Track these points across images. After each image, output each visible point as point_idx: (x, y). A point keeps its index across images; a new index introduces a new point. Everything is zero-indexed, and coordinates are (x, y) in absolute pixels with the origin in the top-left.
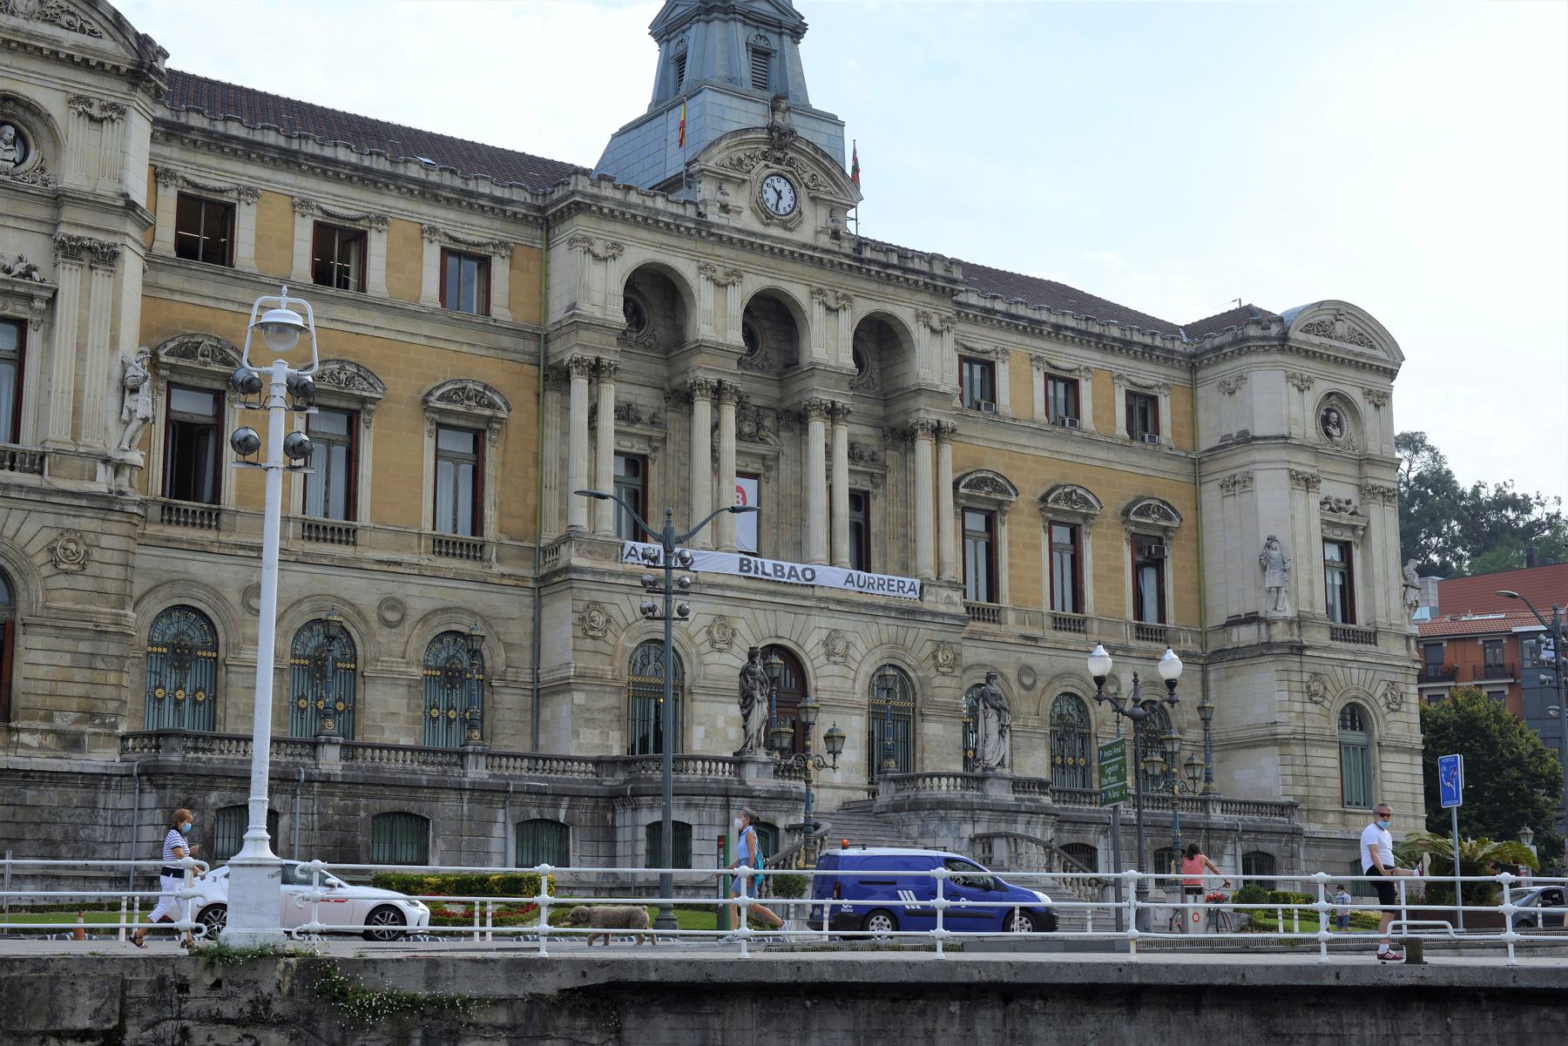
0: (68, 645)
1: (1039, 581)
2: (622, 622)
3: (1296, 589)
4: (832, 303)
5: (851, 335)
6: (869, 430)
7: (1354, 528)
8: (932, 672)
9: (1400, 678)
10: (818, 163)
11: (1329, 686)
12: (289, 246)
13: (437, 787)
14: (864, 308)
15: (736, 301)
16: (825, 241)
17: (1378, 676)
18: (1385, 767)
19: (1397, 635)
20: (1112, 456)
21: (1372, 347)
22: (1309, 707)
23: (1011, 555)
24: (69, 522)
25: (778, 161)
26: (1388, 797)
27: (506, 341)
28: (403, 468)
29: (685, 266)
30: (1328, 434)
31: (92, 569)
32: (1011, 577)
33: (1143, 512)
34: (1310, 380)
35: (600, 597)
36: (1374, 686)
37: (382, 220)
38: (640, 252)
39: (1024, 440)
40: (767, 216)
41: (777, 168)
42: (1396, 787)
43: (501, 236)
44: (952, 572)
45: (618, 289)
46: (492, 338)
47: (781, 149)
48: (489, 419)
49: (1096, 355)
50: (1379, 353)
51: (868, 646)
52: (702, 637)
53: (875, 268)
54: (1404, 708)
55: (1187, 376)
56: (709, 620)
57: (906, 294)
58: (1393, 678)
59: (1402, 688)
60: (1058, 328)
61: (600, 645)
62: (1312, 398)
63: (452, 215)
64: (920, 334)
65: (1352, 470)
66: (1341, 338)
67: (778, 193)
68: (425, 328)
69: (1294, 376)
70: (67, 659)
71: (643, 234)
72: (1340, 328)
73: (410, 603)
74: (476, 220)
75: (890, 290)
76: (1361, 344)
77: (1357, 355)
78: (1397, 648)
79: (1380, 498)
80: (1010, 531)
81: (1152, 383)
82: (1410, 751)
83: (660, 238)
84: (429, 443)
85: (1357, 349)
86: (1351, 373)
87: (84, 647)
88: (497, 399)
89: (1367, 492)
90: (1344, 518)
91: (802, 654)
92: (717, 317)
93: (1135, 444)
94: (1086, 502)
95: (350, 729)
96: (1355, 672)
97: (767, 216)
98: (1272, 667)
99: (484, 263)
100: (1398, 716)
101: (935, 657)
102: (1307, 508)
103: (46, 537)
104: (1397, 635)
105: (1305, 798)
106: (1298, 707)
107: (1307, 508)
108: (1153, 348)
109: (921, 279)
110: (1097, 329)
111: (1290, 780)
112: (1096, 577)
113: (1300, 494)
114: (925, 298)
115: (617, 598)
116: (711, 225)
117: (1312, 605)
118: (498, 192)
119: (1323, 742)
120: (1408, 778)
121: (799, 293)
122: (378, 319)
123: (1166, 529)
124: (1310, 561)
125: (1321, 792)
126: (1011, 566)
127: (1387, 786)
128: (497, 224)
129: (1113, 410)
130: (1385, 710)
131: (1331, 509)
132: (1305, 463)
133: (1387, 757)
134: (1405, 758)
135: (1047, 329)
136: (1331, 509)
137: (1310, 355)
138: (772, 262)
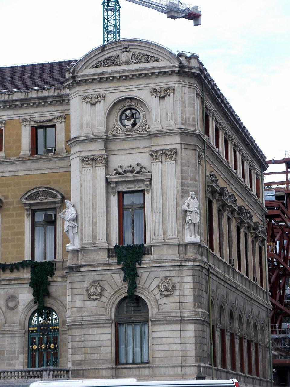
3: (82, 230)
7: (143, 181)
9: (174, 274)
11: (107, 287)
17: (153, 275)
18: (155, 335)
19: (170, 245)
20: (19, 168)
21: (158, 60)
22: (88, 303)
26: (157, 355)
30: (124, 126)
33: (35, 196)
34: (100, 96)
42: (166, 348)
49: (10, 112)
50: (163, 63)
54: (177, 293)
58: (167, 274)
59: (176, 280)
62: (102, 108)
65: (144, 143)
66: (127, 63)
69: (87, 96)
72: (124, 57)
76: (147, 61)
77: (137, 70)
78: (171, 254)
79: (164, 158)
81: (50, 118)
82: (182, 321)
85: (136, 66)
86: (141, 82)
89: (155, 155)
90: (129, 177)
93: (33, 157)
100: (171, 299)
102: (94, 177)
104: (170, 245)
105: (80, 363)
106: (78, 304)
107: (94, 177)
110: (6, 98)
113: (88, 171)
117: (95, 237)
119: (97, 324)
120: (178, 341)
123: (55, 203)
124: (94, 209)
125: (95, 357)
127: (156, 348)
129: (20, 141)
130: (158, 297)
131: (119, 174)
132: (97, 149)
133: (156, 328)
134: (177, 327)
136: (119, 174)
137: (101, 79)
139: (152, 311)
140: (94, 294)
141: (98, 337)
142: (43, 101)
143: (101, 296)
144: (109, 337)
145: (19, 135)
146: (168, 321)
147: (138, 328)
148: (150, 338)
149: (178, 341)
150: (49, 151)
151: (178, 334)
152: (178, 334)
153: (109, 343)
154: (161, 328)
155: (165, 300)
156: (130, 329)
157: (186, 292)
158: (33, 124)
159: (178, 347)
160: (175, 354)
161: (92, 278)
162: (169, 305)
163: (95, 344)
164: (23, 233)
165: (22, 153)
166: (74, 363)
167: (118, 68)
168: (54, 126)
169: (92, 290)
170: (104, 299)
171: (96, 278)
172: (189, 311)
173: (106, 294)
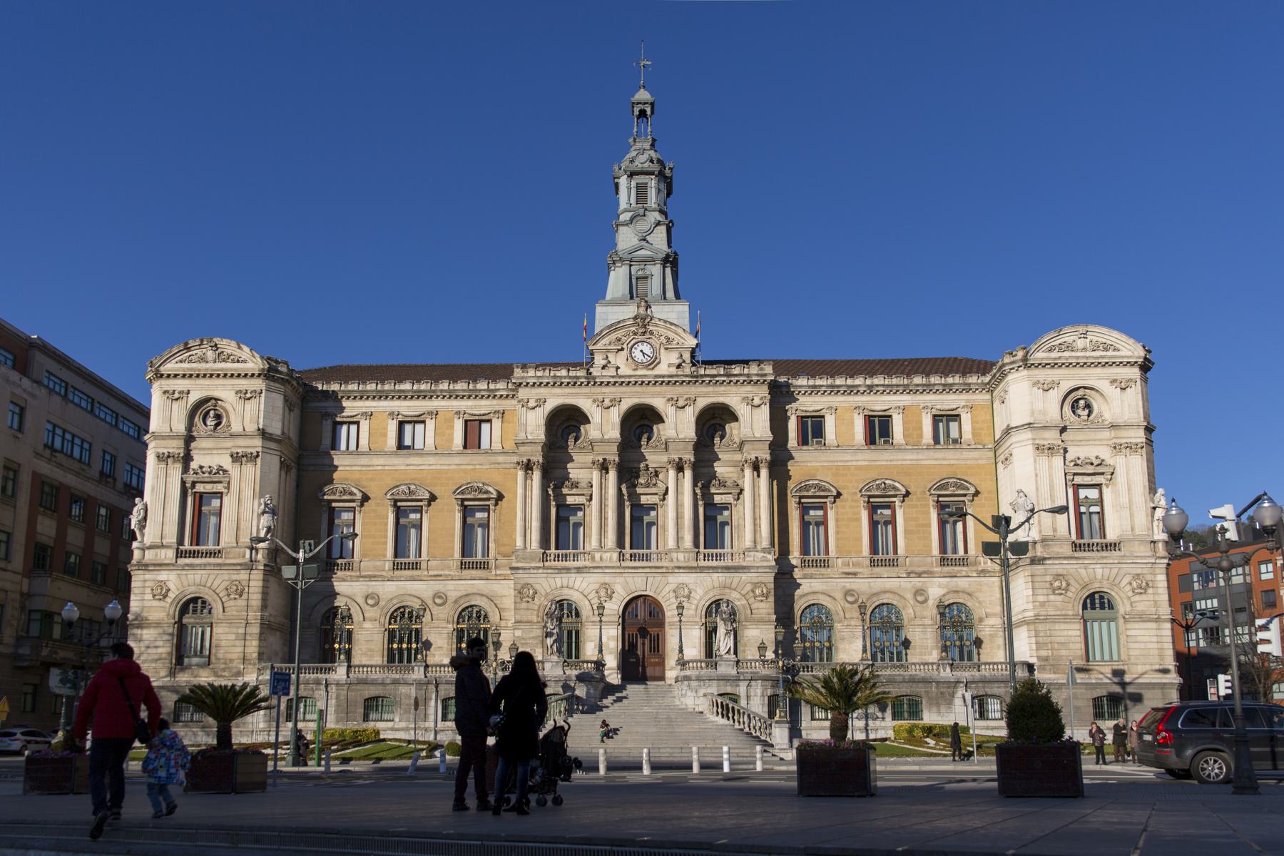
0: (235, 630)
1: (860, 539)
2: (543, 592)
4: (681, 403)
5: (693, 420)
6: (731, 469)
8: (752, 600)
10: (669, 329)
11: (1072, 582)
12: (385, 435)
13: (396, 682)
14: (702, 403)
15: (615, 416)
16: (673, 370)
18: (1129, 633)
20: (920, 457)
22: (1052, 597)
23: (837, 526)
24: (234, 577)
25: (644, 333)
26: (1132, 653)
27: (501, 459)
28: (440, 528)
29: (585, 404)
31: (245, 596)
32: (837, 539)
35: (530, 581)
36: (1119, 579)
37: (430, 413)
38: (556, 398)
39: (849, 457)
40: (638, 365)
41: (641, 338)
42: (1142, 646)
43: (497, 408)
44: (765, 543)
45: (542, 422)
46: (493, 459)
47: (645, 326)
48: (488, 499)
52: (593, 595)
53: (707, 379)
54: (1150, 591)
55: (988, 396)
56: (596, 586)
57: (733, 389)
58: (1139, 571)
59: (1149, 577)
60: (870, 387)
61: (530, 605)
63: (470, 403)
64: (742, 410)
67: (642, 351)
68: (457, 460)
70: (233, 637)
71: (557, 390)
73: (449, 594)
74: (484, 402)
75: (722, 388)
80: (837, 513)
82: (1158, 620)
83: (568, 390)
84: (458, 517)
87: (242, 631)
88: (490, 489)
91: (659, 598)
92: (604, 426)
94: (895, 488)
95: (349, 659)
96: (1099, 571)
97: (638, 365)
98: (1022, 574)
99: (489, 421)
100: (1144, 597)
101: (753, 591)
103: (225, 584)
105: (1046, 659)
106: (1041, 598)
108: (951, 385)
109: (742, 379)
111: (1034, 646)
112: (906, 532)
114: (749, 388)
115: (539, 581)
116: (595, 378)
118: (492, 386)
119: (1064, 618)
120: (1154, 639)
121: (659, 403)
122: (431, 460)
125: (1063, 653)
126: (837, 533)
128: (495, 402)
129: (921, 428)
130: (1130, 594)
133: (1129, 626)
134: (1153, 625)
135: (862, 389)
138: (637, 388)
139: (1122, 607)
140: (1060, 588)
141: (1065, 633)
142: (948, 388)
143: (1066, 590)
144: (1078, 633)
145: (920, 422)
146: (1142, 618)
147: (1104, 625)
148: (1123, 637)
149: (1154, 639)
150: (955, 441)
151: (1154, 632)
152: (1154, 632)
153: (1078, 639)
154: (1136, 625)
155: (1137, 598)
156: (1096, 625)
157: (1160, 591)
158: (934, 412)
159: (1155, 646)
160: (1152, 652)
161: (1055, 572)
162: (1143, 604)
163: (1062, 640)
164: (929, 525)
165: (924, 441)
166: (1039, 658)
167: (1074, 354)
168: (958, 416)
169: (1057, 584)
170: (1069, 594)
171: (1060, 572)
172: (1165, 611)
173: (1071, 588)
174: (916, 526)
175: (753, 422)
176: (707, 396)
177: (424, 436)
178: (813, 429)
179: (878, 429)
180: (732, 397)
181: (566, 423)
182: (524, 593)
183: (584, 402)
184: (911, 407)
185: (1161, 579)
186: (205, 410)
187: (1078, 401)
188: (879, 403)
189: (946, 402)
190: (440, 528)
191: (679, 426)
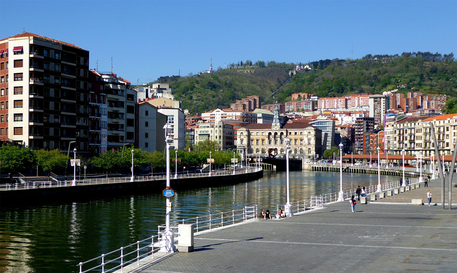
28: (260, 142)
38: (269, 132)
51: (280, 148)
67: (276, 127)
92: (273, 134)
174: (298, 142)
175: (285, 134)
176: (281, 131)
177: (259, 134)
178: (290, 133)
179: (296, 133)
180: (283, 131)
181: (270, 134)
182: (267, 148)
183: (271, 132)
184: (299, 132)
185: (314, 147)
186: (242, 133)
187: (309, 133)
188: (296, 131)
189: (301, 131)
190: (260, 142)
191: (279, 134)
